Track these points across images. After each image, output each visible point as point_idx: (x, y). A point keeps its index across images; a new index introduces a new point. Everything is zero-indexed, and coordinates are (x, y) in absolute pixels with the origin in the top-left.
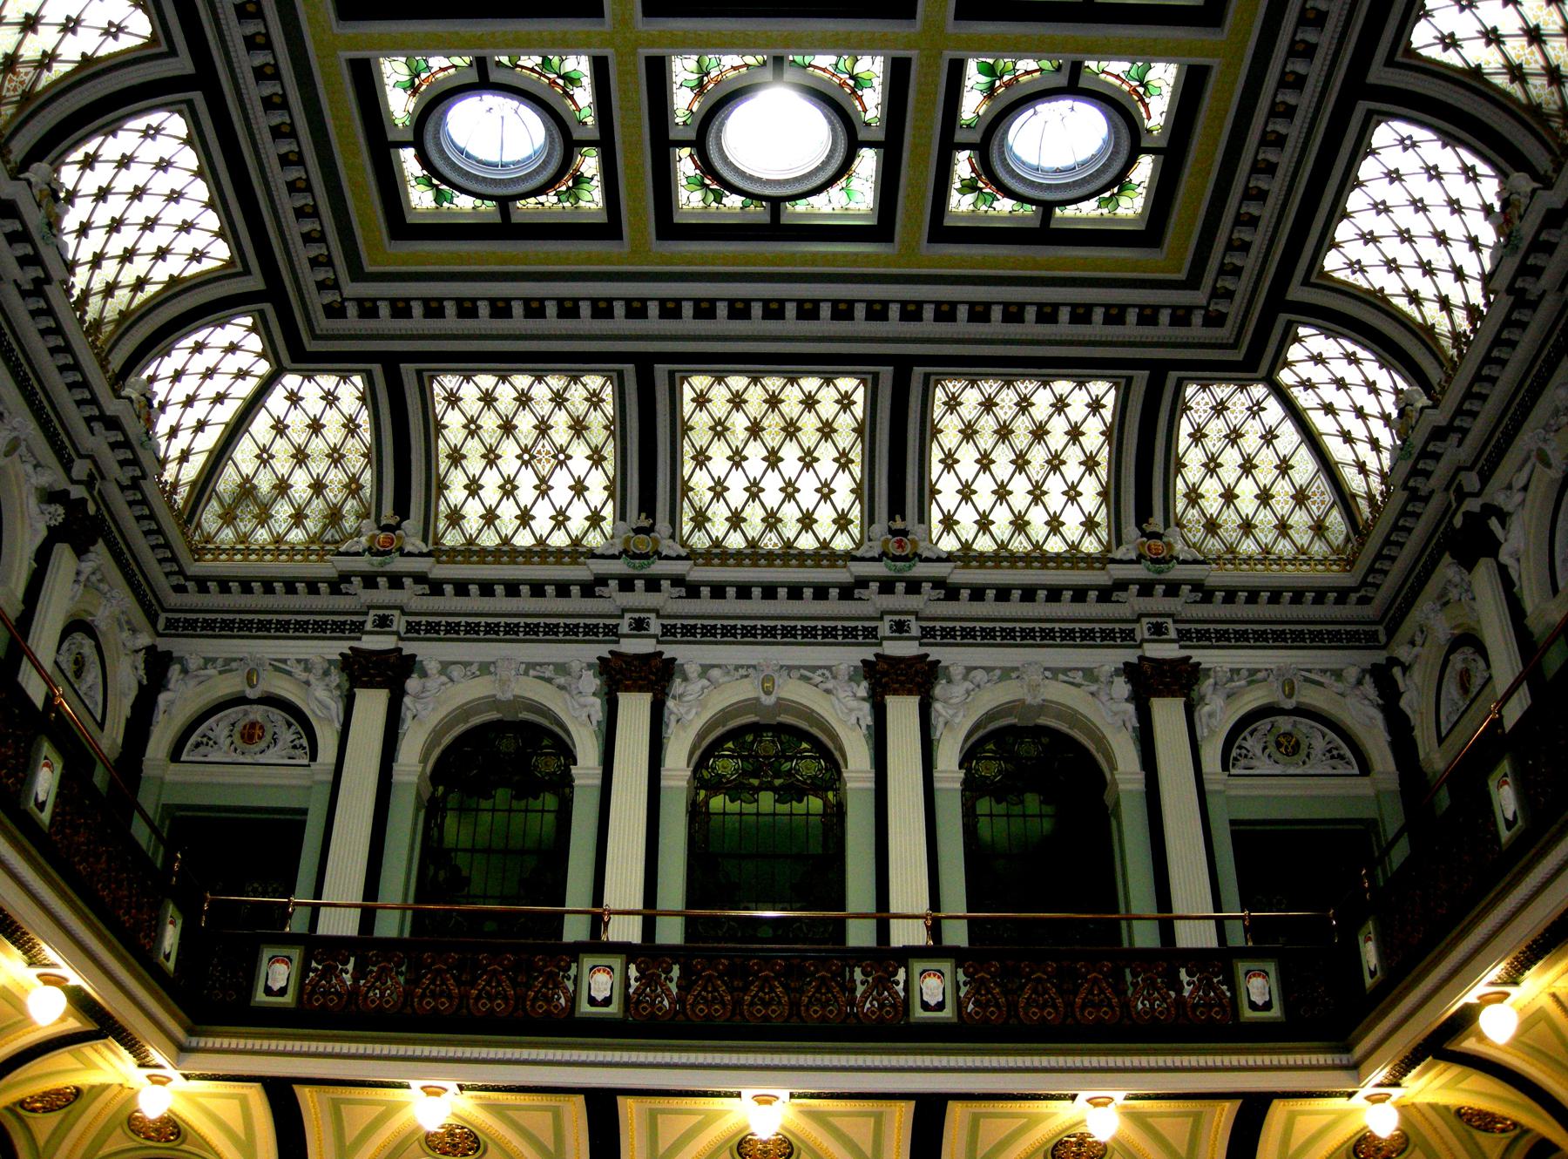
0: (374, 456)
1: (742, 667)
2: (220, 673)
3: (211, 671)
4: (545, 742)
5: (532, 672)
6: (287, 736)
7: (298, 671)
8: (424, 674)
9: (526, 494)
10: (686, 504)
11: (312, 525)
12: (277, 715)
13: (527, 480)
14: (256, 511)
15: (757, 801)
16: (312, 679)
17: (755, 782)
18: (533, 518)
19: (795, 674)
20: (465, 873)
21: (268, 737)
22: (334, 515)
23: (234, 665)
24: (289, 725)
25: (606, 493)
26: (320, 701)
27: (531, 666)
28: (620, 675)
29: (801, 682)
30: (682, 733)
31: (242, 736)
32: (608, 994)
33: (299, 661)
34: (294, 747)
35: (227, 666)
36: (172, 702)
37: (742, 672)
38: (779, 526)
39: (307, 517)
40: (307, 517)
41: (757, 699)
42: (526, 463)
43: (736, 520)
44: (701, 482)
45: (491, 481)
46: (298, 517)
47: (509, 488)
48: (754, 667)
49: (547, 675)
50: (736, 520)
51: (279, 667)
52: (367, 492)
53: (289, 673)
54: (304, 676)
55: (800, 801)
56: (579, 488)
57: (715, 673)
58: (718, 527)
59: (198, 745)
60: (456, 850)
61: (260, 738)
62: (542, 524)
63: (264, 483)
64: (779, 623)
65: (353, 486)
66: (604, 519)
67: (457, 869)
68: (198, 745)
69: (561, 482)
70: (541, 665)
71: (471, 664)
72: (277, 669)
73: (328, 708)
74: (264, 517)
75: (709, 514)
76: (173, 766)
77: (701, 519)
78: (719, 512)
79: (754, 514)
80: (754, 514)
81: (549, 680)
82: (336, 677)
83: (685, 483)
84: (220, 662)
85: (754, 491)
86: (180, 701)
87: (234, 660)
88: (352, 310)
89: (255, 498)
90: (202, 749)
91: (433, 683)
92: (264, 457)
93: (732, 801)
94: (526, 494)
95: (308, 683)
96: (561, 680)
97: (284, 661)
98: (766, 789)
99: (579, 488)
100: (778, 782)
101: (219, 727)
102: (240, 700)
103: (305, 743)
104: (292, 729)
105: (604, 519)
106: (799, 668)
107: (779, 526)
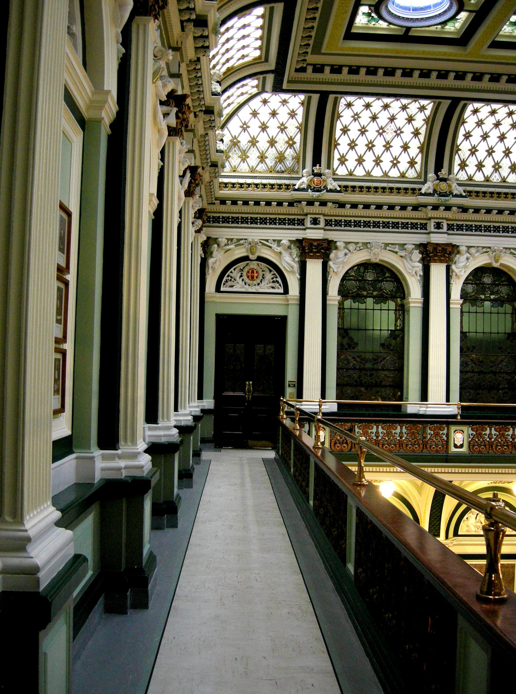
0: (304, 128)
1: (485, 247)
2: (236, 246)
3: (232, 246)
4: (387, 275)
5: (388, 248)
6: (269, 276)
7: (274, 246)
8: (336, 248)
9: (379, 149)
10: (457, 157)
11: (270, 162)
12: (263, 265)
13: (379, 143)
14: (240, 154)
15: (483, 306)
16: (283, 252)
17: (483, 297)
18: (382, 161)
19: (508, 251)
20: (355, 340)
21: (260, 277)
22: (281, 158)
23: (242, 242)
24: (270, 271)
25: (418, 150)
26: (288, 262)
27: (387, 245)
28: (430, 254)
29: (511, 255)
30: (457, 281)
31: (248, 277)
32: (462, 443)
33: (274, 241)
34: (273, 282)
35: (238, 242)
36: (216, 262)
37: (485, 250)
38: (500, 170)
39: (267, 158)
40: (267, 158)
41: (490, 264)
42: (380, 134)
43: (480, 166)
44: (465, 147)
45: (362, 142)
46: (262, 158)
47: (370, 146)
48: (490, 248)
49: (396, 250)
50: (480, 166)
51: (265, 243)
52: (297, 146)
53: (271, 247)
54: (279, 249)
55: (502, 306)
56: (405, 147)
57: (473, 250)
58: (471, 169)
59: (226, 281)
60: (351, 329)
61: (257, 277)
62: (386, 165)
63: (244, 140)
64: (501, 225)
65: (291, 143)
66: (416, 163)
67: (351, 339)
68: (226, 281)
69: (397, 144)
70: (392, 244)
71: (358, 243)
72: (264, 244)
73: (292, 267)
74: (244, 157)
75: (467, 163)
76: (219, 295)
77: (463, 165)
78: (472, 162)
79: (489, 164)
80: (489, 164)
81: (396, 253)
82: (295, 251)
83: (458, 146)
84: (235, 241)
85: (490, 152)
86: (218, 261)
87: (242, 239)
88: (310, 69)
89: (239, 147)
90: (229, 283)
91: (341, 254)
92: (245, 127)
93: (472, 306)
94: (379, 149)
95: (280, 253)
96: (403, 253)
97: (267, 241)
98: (487, 300)
99: (405, 147)
100: (492, 297)
101: (235, 273)
102: (245, 258)
103: (280, 281)
104: (272, 273)
105: (416, 163)
106: (510, 249)
107: (500, 170)
